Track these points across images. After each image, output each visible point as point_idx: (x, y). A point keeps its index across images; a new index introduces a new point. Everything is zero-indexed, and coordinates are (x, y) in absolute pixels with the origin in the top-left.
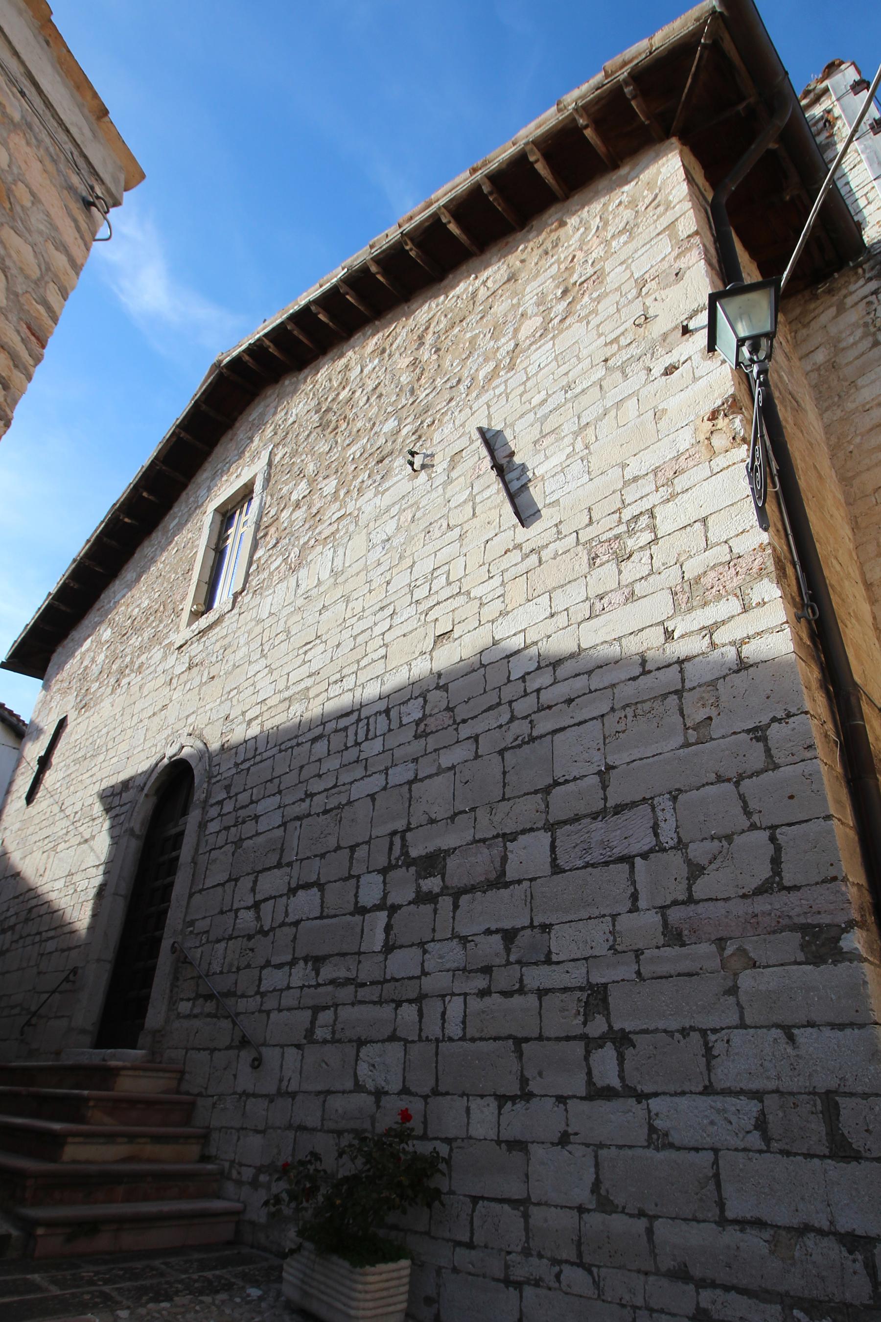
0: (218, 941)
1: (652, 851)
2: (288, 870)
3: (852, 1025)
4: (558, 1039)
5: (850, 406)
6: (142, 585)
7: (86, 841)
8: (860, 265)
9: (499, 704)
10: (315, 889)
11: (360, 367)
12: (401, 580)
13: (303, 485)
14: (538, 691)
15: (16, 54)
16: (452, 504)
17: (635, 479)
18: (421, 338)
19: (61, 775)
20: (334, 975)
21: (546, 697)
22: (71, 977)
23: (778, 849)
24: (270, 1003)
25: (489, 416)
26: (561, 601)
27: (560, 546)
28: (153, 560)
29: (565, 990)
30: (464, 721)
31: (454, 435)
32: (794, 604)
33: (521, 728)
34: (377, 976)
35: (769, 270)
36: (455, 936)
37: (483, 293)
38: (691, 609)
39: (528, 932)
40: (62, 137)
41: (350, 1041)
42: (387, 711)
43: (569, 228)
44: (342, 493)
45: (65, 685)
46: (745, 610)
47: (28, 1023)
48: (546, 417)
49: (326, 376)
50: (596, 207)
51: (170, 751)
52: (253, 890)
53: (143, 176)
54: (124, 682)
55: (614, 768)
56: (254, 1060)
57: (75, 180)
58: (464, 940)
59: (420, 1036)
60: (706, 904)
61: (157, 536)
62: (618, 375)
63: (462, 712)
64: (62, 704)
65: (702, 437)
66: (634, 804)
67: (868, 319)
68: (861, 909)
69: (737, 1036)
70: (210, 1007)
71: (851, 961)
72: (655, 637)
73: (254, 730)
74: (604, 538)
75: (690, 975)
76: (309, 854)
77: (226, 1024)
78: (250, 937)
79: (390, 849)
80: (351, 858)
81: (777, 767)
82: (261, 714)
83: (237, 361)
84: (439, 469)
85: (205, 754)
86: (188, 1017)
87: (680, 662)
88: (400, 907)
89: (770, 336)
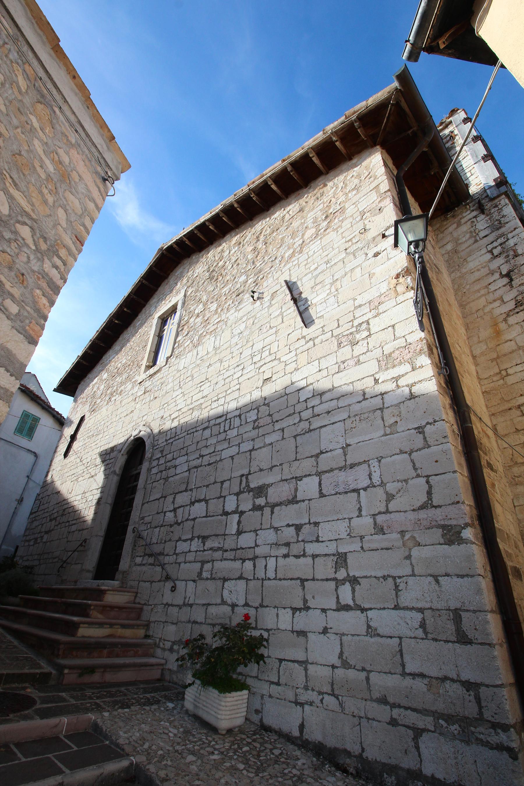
0: (156, 527)
1: (368, 487)
2: (190, 493)
3: (467, 576)
4: (322, 580)
6: (123, 353)
7: (92, 476)
9: (294, 413)
10: (204, 502)
11: (229, 251)
12: (247, 352)
13: (201, 306)
14: (313, 407)
15: (74, 113)
16: (272, 317)
17: (360, 306)
18: (258, 237)
19: (81, 444)
20: (213, 545)
21: (317, 410)
22: (83, 544)
23: (430, 487)
24: (181, 559)
25: (290, 275)
26: (324, 364)
27: (324, 337)
28: (128, 341)
29: (326, 555)
30: (277, 421)
31: (274, 284)
32: (437, 367)
33: (304, 425)
34: (233, 546)
35: (425, 207)
36: (272, 527)
37: (287, 217)
38: (387, 369)
39: (308, 526)
40: (93, 149)
41: (220, 579)
42: (240, 416)
43: (328, 187)
44: (219, 310)
45: (85, 400)
46: (413, 369)
47: (62, 566)
48: (317, 276)
49: (212, 254)
50: (341, 177)
51: (134, 433)
52: (173, 502)
53: (130, 166)
54: (113, 399)
55: (350, 445)
56: (173, 587)
57: (99, 169)
58: (276, 529)
59: (254, 577)
60: (395, 514)
61: (130, 329)
62: (352, 256)
63: (276, 417)
64: (83, 409)
65: (392, 287)
66: (360, 464)
68: (472, 517)
69: (411, 580)
70: (151, 560)
71: (467, 543)
72: (370, 382)
73: (175, 424)
74: (345, 334)
75: (387, 549)
76: (201, 485)
77: (159, 569)
78: (171, 526)
79: (241, 483)
80: (221, 487)
81: (429, 446)
82: (179, 416)
83: (170, 248)
84: (266, 299)
85: (151, 435)
86: (140, 565)
87: (382, 394)
88: (245, 512)
89: (424, 240)
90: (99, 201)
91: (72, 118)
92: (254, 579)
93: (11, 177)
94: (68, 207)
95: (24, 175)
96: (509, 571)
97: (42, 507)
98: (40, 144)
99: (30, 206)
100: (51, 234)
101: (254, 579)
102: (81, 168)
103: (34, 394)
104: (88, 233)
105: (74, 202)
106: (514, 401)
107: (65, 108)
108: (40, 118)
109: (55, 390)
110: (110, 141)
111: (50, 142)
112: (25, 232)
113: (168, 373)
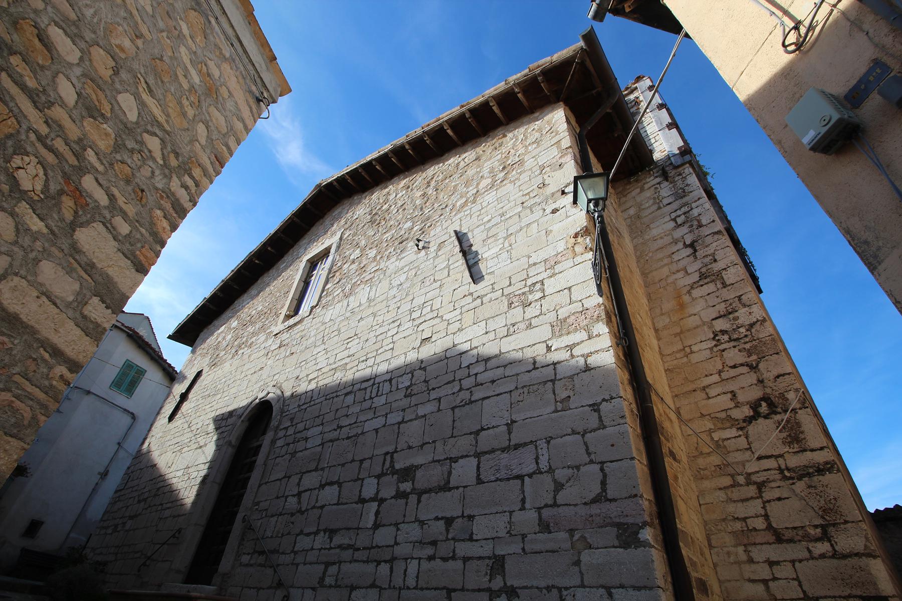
0: (272, 516)
1: (534, 473)
2: (321, 472)
3: (645, 587)
4: (474, 590)
5: (647, 237)
6: (260, 298)
7: (201, 447)
8: (652, 170)
9: (454, 380)
10: (336, 486)
11: (396, 194)
12: (406, 307)
13: (358, 251)
14: (476, 374)
15: (232, 26)
16: (437, 269)
17: (535, 264)
18: (428, 183)
19: (193, 405)
20: (342, 542)
21: (480, 378)
22: (177, 535)
23: (605, 476)
24: (300, 559)
25: (461, 225)
26: (492, 325)
27: (493, 296)
28: (268, 285)
29: (480, 558)
30: (433, 389)
31: (442, 233)
32: (616, 337)
33: (465, 395)
34: (368, 544)
35: (607, 168)
36: (417, 520)
37: (462, 164)
38: (561, 336)
39: (460, 520)
40: (250, 67)
41: (346, 587)
42: (390, 380)
43: (508, 138)
44: (378, 258)
45: (205, 351)
46: (590, 338)
47: (144, 564)
48: (490, 228)
49: (377, 197)
50: (522, 130)
51: (261, 395)
52: (298, 484)
53: (290, 91)
54: (240, 352)
55: (515, 422)
56: (285, 596)
57: (254, 88)
58: (422, 523)
59: (390, 585)
60: (564, 508)
61: (273, 272)
62: (528, 210)
63: (433, 384)
64: (201, 362)
65: (570, 246)
66: (525, 444)
67: (655, 196)
68: (651, 515)
69: (580, 592)
70: (261, 559)
71: (645, 547)
72: (542, 349)
73: (313, 386)
74: (517, 293)
75: (553, 552)
76: (335, 463)
77: (269, 571)
78: (292, 515)
79: (384, 463)
80: (360, 467)
81: (605, 427)
82: (318, 377)
83: (330, 185)
84: (432, 250)
85: (281, 398)
86: (247, 565)
87: (554, 364)
88: (386, 500)
89: (604, 199)
90: (249, 122)
91: (230, 31)
92: (390, 588)
93: (146, 82)
94: (210, 124)
95: (162, 82)
96: (694, 584)
97: (130, 484)
98: (187, 52)
99: (164, 117)
100: (185, 150)
101: (390, 588)
102: (233, 83)
103: (143, 341)
104: (231, 155)
105: (218, 118)
106: (699, 382)
107: (222, 20)
108: (192, 26)
109: (170, 337)
110: (271, 61)
111: (199, 52)
112: (154, 144)
113: (310, 325)
